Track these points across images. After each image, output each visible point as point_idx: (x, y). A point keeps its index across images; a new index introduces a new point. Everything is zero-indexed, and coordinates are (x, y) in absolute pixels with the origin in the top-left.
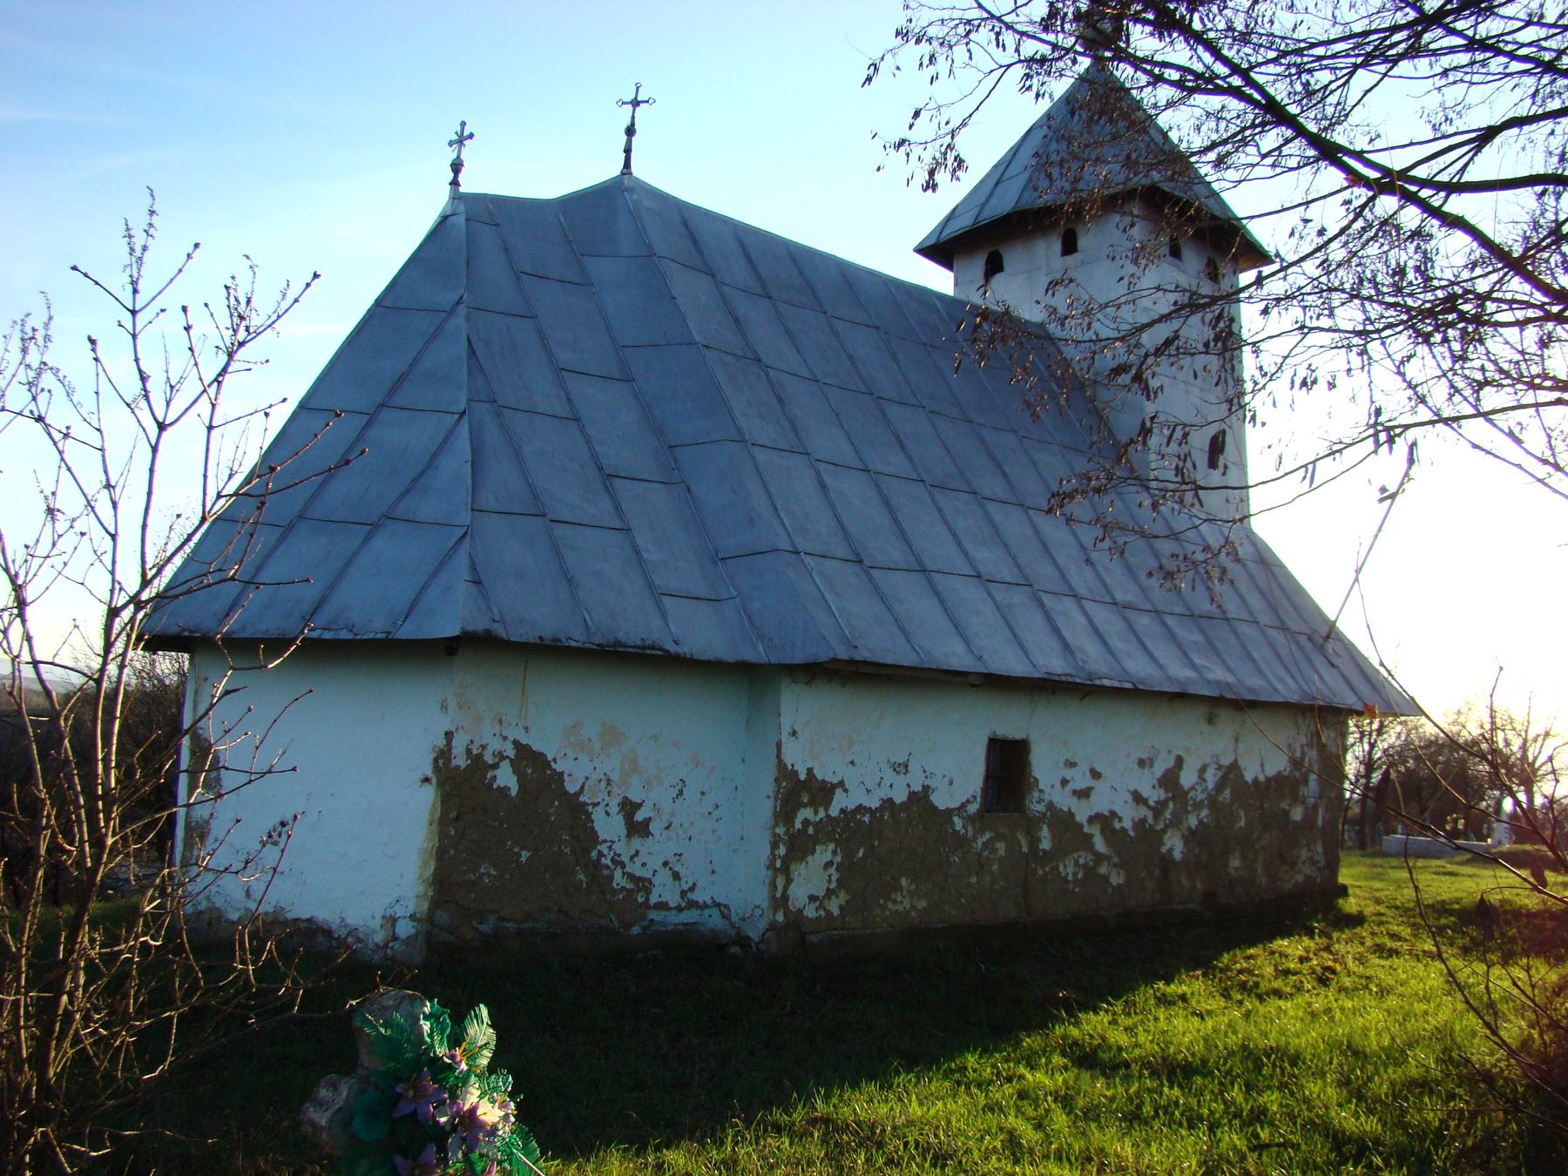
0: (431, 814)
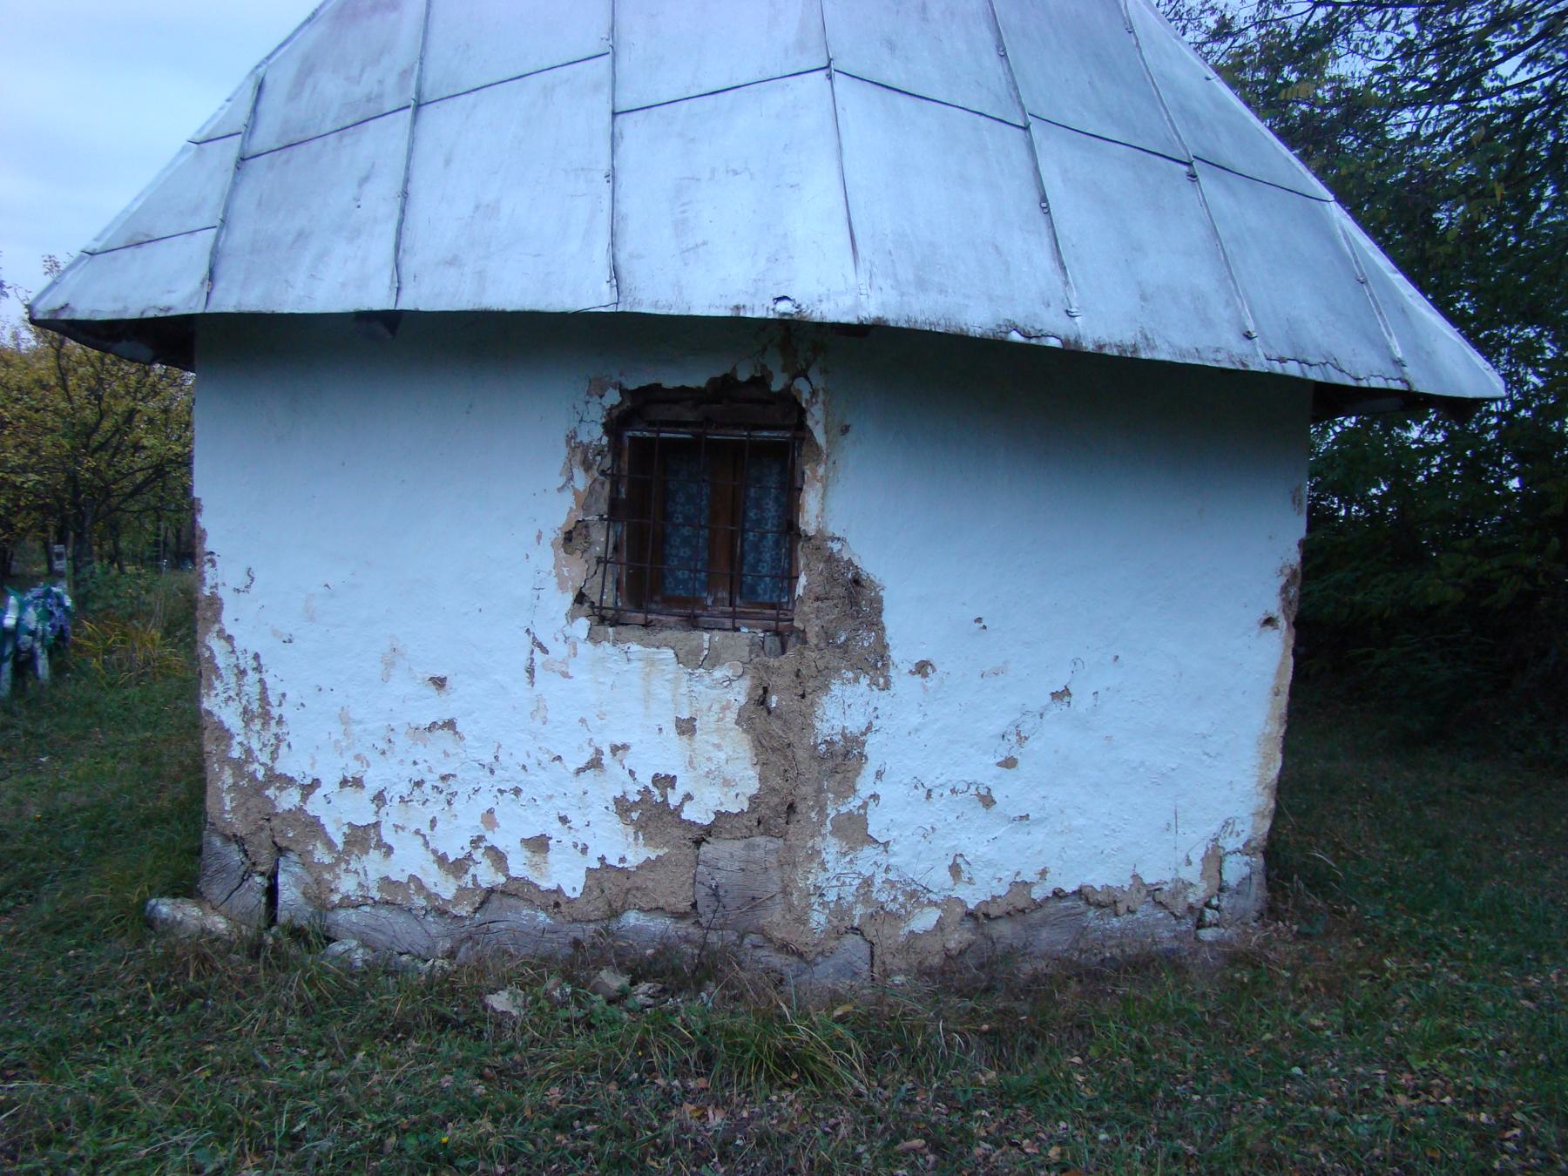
0: (1279, 674)
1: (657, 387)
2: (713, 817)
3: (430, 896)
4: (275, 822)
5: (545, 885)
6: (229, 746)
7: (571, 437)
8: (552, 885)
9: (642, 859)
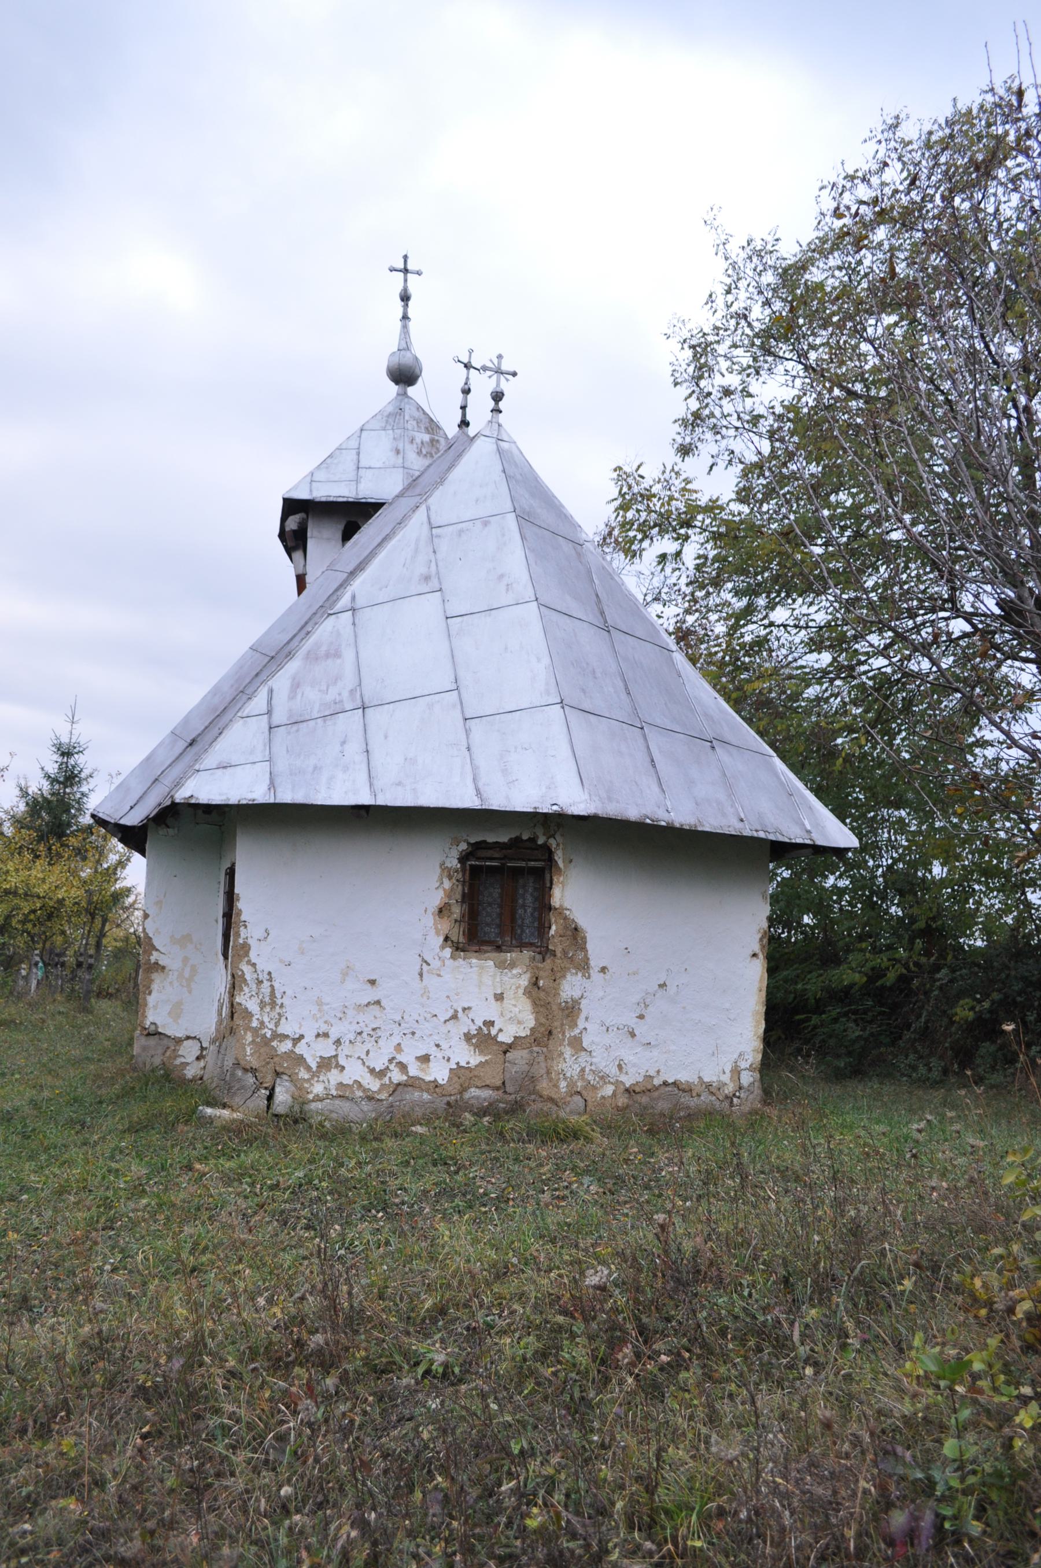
0: (761, 981)
1: (484, 842)
3: (365, 1090)
4: (276, 1059)
6: (250, 1021)
7: (442, 864)
8: (432, 1079)
9: (477, 1062)
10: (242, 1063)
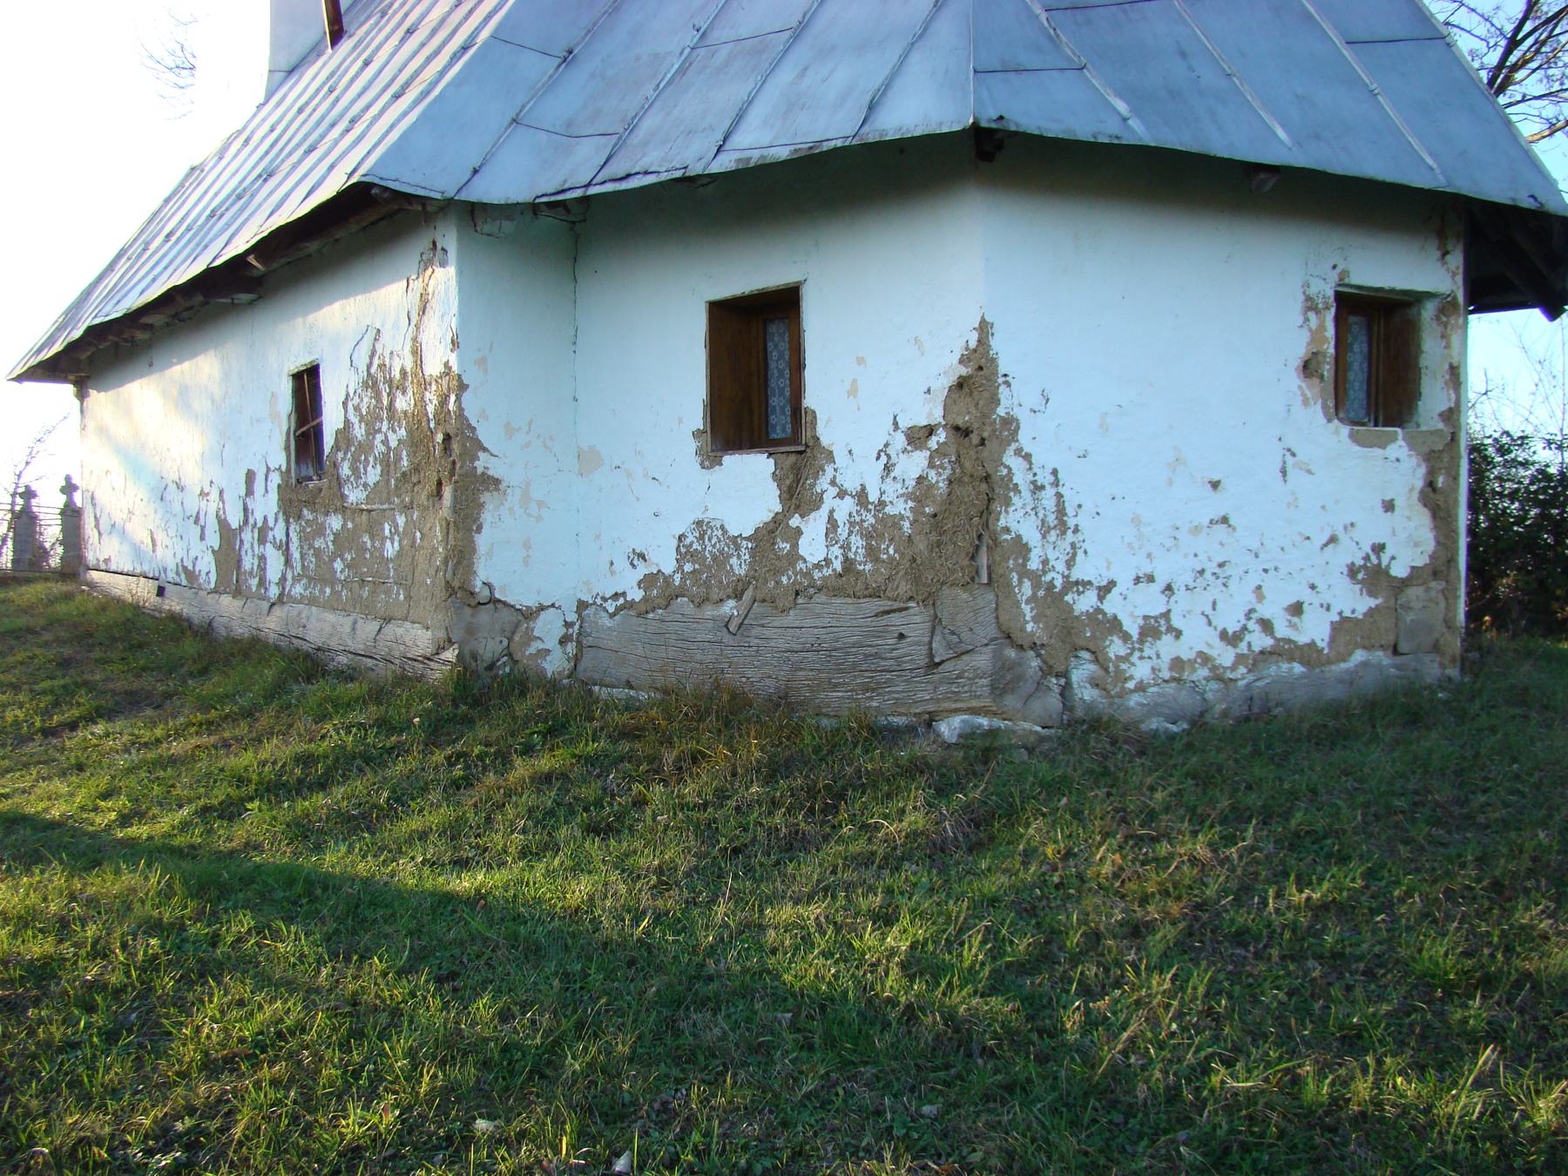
2: (1409, 570)
3: (1214, 668)
5: (1302, 639)
6: (1026, 559)
10: (1016, 635)
